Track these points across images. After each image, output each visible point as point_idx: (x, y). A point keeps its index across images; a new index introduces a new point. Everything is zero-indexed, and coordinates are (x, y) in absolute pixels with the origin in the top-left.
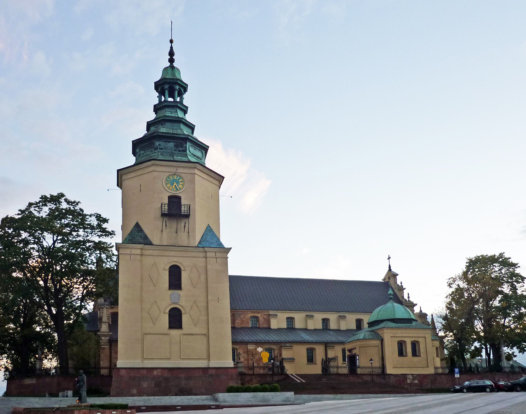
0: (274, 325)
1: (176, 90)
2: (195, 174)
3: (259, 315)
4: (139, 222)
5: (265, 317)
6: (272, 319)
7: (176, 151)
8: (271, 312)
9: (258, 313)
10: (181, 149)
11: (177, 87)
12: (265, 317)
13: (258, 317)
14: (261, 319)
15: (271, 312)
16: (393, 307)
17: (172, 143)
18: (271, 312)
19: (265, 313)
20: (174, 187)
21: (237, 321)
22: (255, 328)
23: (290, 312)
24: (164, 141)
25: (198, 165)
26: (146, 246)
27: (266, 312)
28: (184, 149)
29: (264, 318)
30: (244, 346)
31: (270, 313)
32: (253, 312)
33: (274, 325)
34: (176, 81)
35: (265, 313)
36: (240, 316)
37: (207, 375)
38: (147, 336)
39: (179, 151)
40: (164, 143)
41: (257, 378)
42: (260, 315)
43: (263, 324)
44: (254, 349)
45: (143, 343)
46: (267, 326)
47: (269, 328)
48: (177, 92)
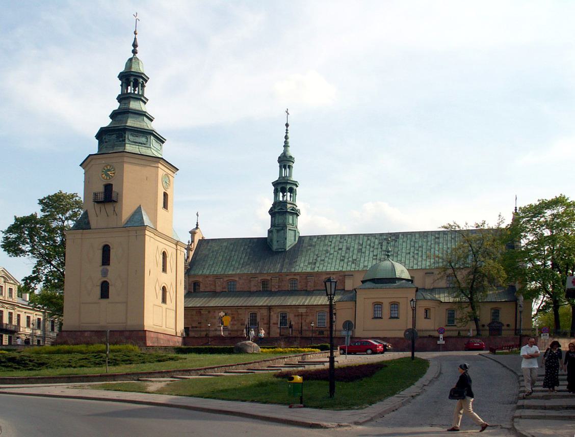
1: (140, 83)
4: (88, 210)
7: (117, 142)
10: (121, 139)
11: (141, 80)
16: (393, 266)
17: (115, 136)
20: (111, 174)
26: (85, 231)
28: (124, 139)
34: (129, 73)
39: (120, 141)
48: (140, 85)
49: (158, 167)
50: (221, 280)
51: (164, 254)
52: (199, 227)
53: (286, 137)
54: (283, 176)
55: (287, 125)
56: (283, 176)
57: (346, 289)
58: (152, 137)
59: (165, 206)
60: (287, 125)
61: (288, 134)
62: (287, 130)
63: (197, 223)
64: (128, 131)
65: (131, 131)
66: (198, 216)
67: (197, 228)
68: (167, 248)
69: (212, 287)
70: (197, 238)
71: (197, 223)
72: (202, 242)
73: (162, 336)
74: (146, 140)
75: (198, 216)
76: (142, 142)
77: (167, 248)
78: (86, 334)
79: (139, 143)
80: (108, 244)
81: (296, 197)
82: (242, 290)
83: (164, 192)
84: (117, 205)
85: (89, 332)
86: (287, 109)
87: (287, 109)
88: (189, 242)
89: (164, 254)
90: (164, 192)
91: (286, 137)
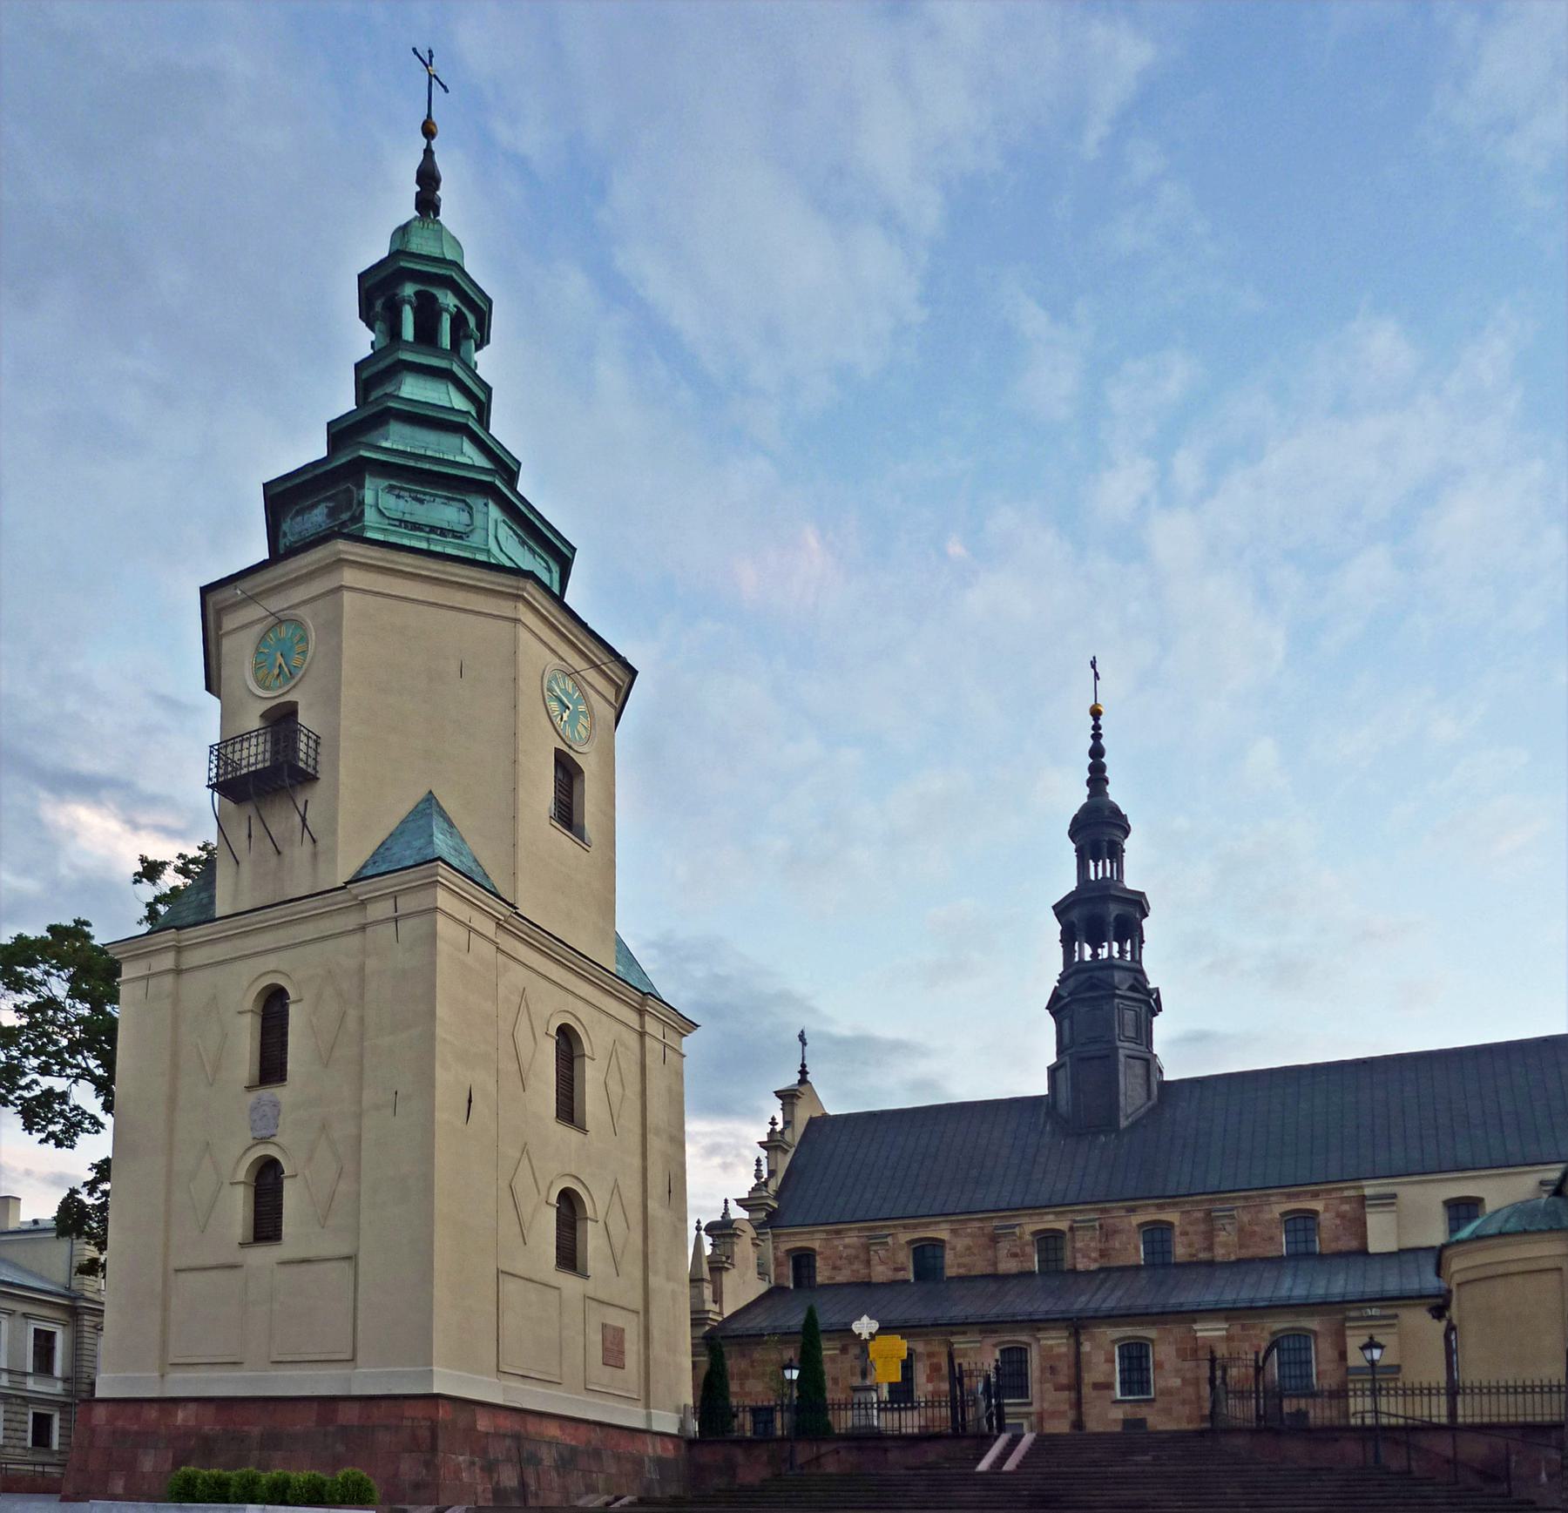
0: (1381, 1234)
2: (520, 620)
3: (1317, 1205)
5: (1346, 1207)
6: (1371, 1213)
8: (1370, 1189)
9: (1315, 1195)
12: (1346, 1207)
13: (1315, 1213)
14: (1327, 1219)
15: (1369, 1186)
18: (1369, 1186)
19: (1346, 1193)
21: (1222, 1237)
22: (1302, 1256)
23: (1460, 1175)
24: (298, 513)
25: (530, 586)
27: (1347, 1188)
29: (1341, 1216)
30: (1178, 1331)
31: (1368, 1192)
32: (1290, 1196)
33: (1381, 1234)
35: (1346, 1193)
36: (1232, 1217)
37: (331, 1428)
38: (182, 1275)
40: (299, 519)
41: (843, 1453)
42: (1324, 1202)
43: (1337, 1239)
44: (1221, 1337)
45: (165, 1307)
46: (1354, 1244)
47: (1363, 1252)
49: (516, 621)
50: (889, 1240)
51: (567, 1040)
52: (809, 1077)
53: (1097, 752)
54: (1093, 878)
55: (1096, 713)
56: (1093, 878)
57: (1371, 1249)
58: (494, 512)
59: (567, 814)
60: (1096, 713)
61: (1102, 741)
62: (1096, 727)
63: (803, 1066)
64: (374, 474)
65: (391, 477)
66: (804, 1044)
67: (803, 1080)
68: (583, 1011)
69: (855, 1267)
70: (802, 1115)
71: (803, 1066)
72: (821, 1125)
73: (553, 1430)
74: (465, 517)
75: (804, 1044)
76: (445, 525)
77: (583, 1011)
78: (181, 1416)
79: (433, 529)
80: (282, 982)
81: (1143, 951)
82: (962, 1271)
83: (557, 751)
84: (315, 799)
85: (192, 1407)
86: (1094, 658)
87: (1094, 658)
88: (773, 1123)
89: (567, 1040)
90: (557, 751)
91: (1097, 752)
